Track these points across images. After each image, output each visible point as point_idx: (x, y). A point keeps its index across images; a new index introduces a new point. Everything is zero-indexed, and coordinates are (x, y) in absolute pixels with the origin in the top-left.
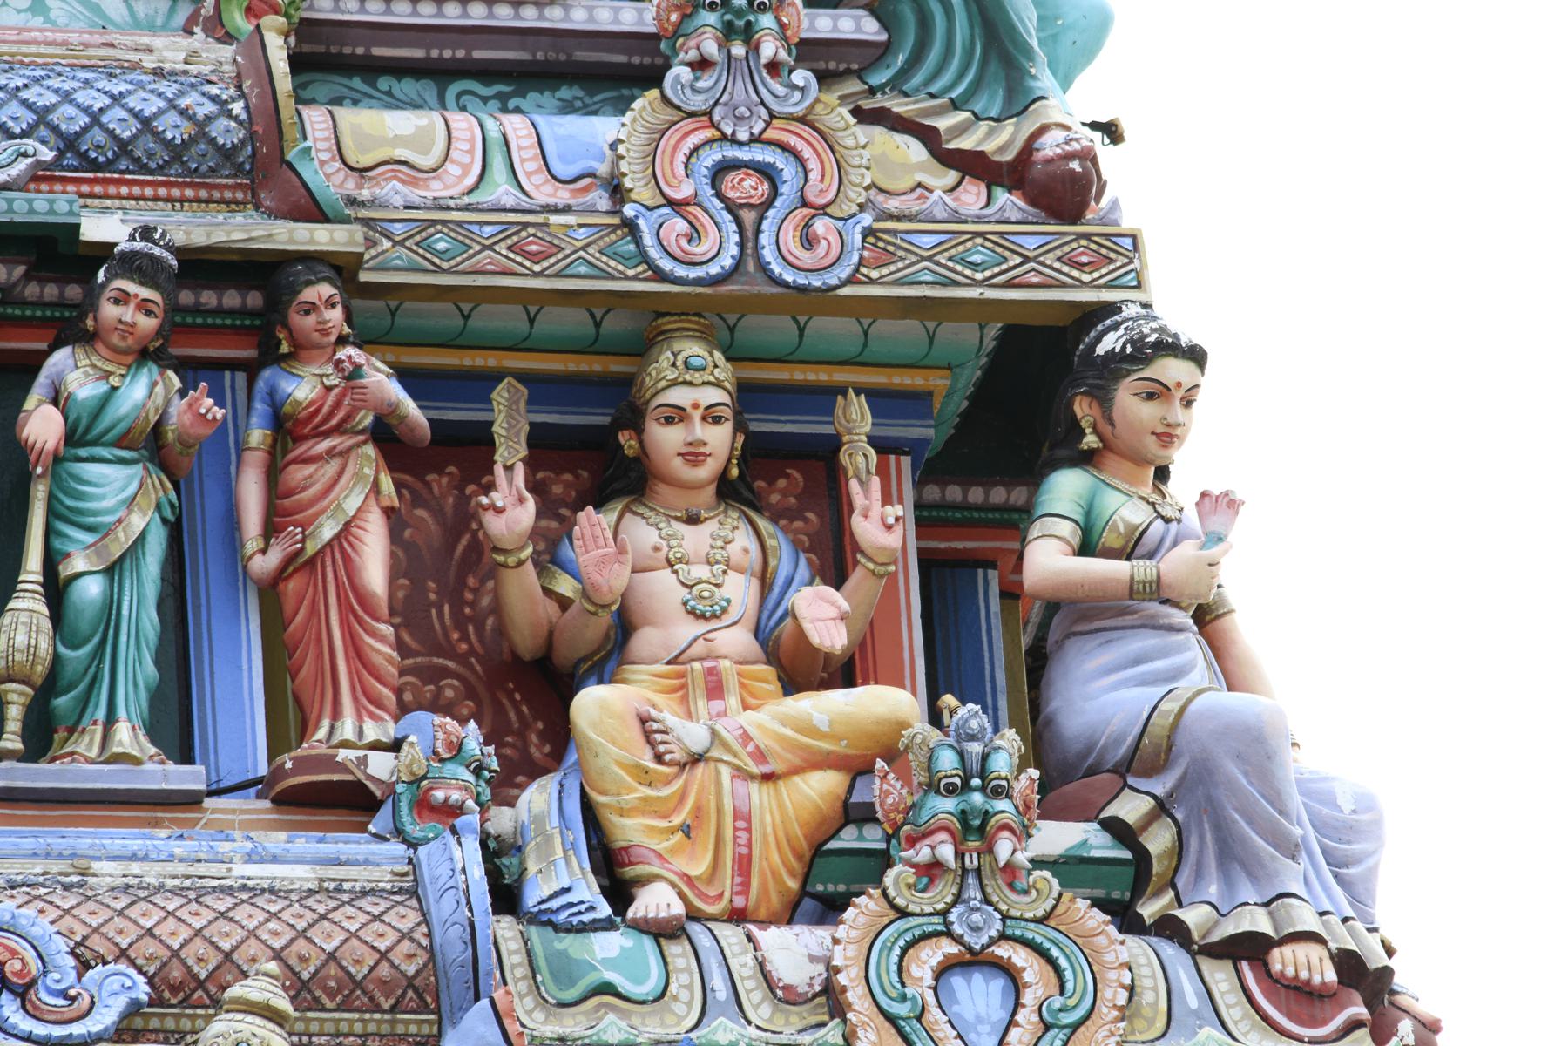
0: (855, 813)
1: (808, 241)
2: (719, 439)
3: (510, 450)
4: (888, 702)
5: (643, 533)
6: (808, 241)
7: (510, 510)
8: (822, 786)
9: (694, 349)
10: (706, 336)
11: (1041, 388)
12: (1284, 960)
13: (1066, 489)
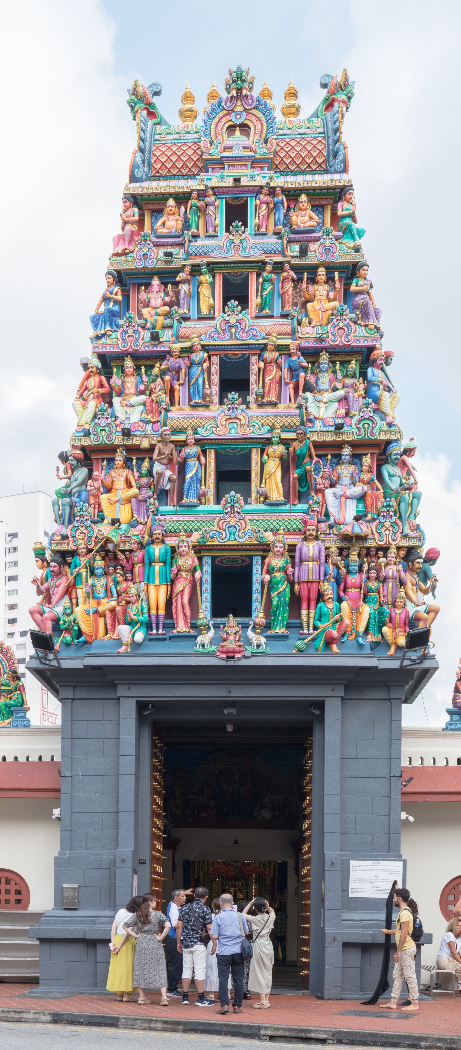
0: (332, 314)
1: (333, 256)
2: (324, 277)
3: (305, 279)
4: (336, 303)
5: (316, 287)
6: (333, 256)
7: (304, 285)
8: (330, 312)
9: (322, 268)
10: (323, 267)
11: (352, 271)
12: (369, 326)
13: (355, 280)
